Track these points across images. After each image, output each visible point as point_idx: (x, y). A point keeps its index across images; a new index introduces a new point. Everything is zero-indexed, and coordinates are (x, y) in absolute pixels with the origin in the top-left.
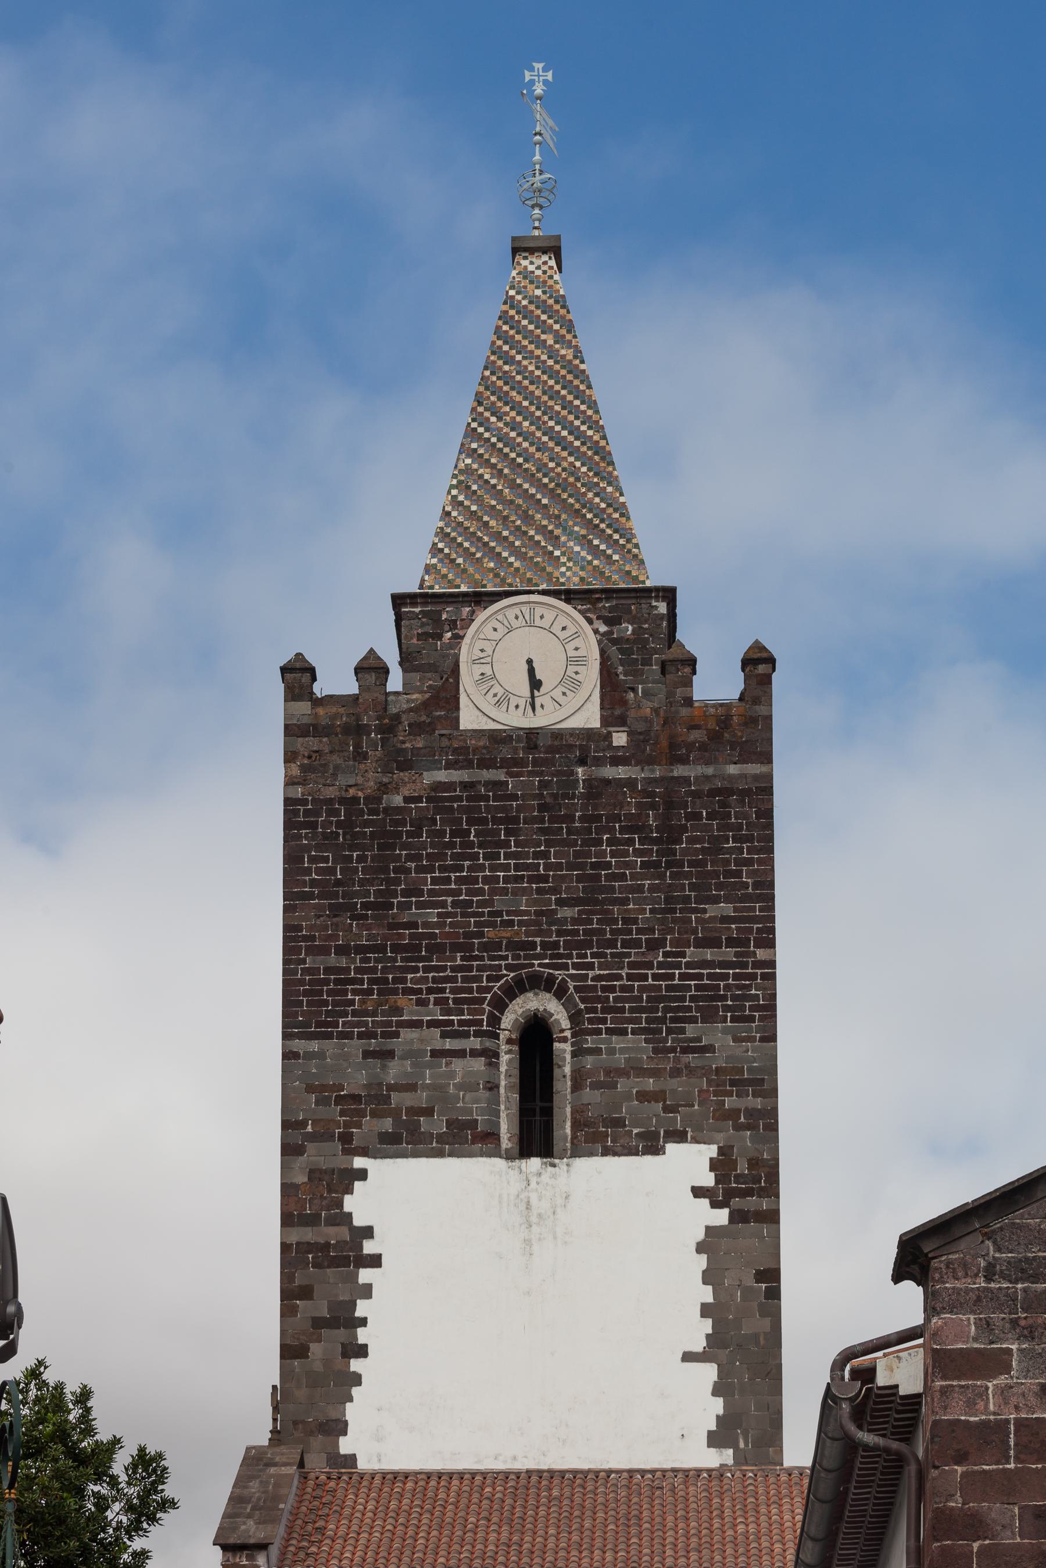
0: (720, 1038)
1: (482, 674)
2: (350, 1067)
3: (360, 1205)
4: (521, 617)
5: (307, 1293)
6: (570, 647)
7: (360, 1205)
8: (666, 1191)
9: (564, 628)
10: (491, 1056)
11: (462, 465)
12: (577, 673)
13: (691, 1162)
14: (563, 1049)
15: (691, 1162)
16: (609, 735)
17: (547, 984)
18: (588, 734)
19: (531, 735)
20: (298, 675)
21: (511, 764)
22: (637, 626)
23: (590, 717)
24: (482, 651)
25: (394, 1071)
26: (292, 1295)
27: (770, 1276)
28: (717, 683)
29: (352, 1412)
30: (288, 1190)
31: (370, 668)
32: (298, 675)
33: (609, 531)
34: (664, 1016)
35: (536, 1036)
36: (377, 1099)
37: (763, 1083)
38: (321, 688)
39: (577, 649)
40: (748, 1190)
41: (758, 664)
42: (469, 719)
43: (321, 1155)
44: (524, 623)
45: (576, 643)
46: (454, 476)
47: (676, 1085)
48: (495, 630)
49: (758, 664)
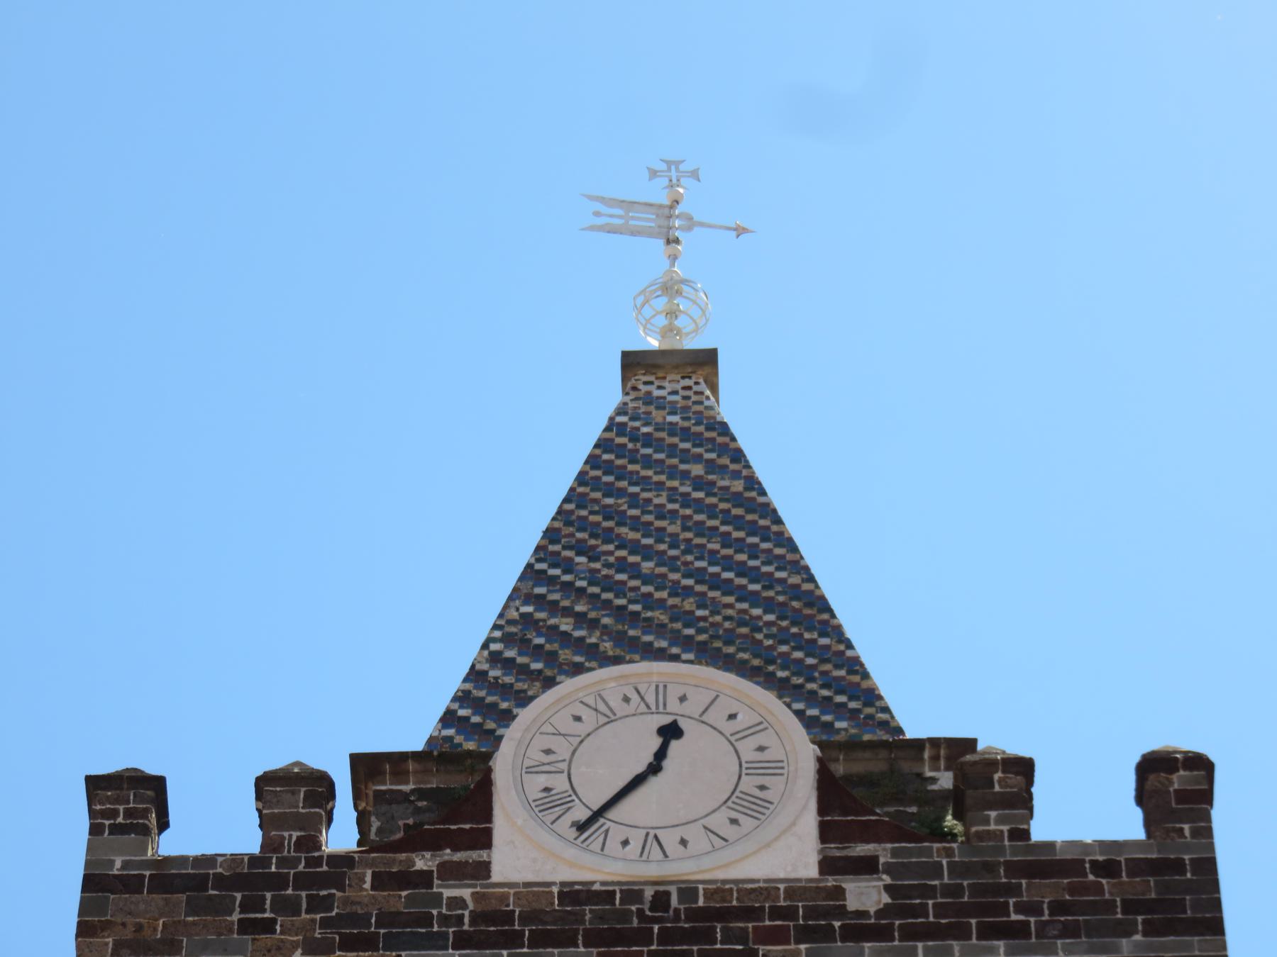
1: (547, 790)
4: (635, 698)
6: (747, 749)
9: (732, 717)
11: (514, 614)
12: (762, 788)
16: (839, 892)
18: (795, 889)
20: (127, 800)
24: (548, 752)
32: (127, 800)
33: (825, 693)
38: (181, 839)
39: (761, 749)
41: (1175, 787)
44: (643, 708)
45: (760, 739)
46: (496, 627)
48: (578, 719)
49: (1175, 787)
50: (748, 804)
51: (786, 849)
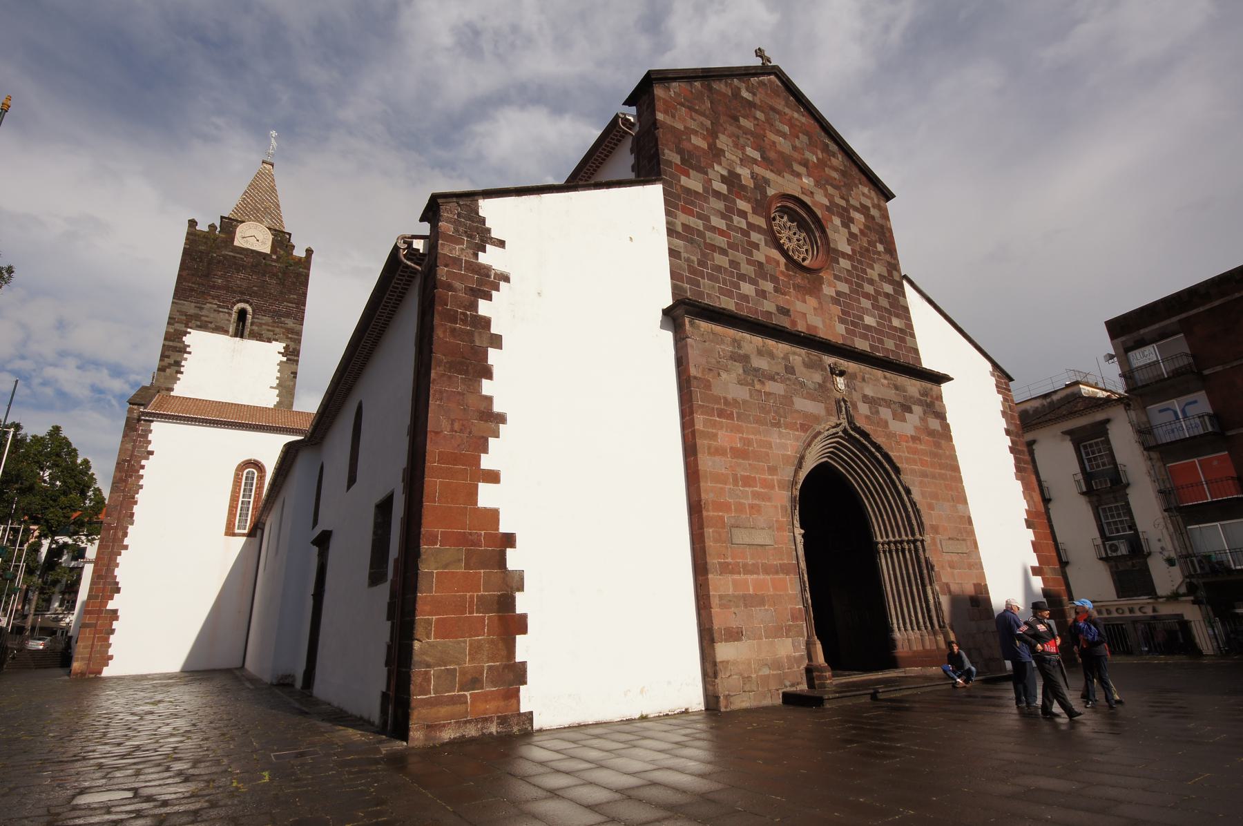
0: (290, 323)
2: (190, 308)
3: (187, 340)
5: (168, 357)
7: (187, 340)
8: (273, 352)
10: (230, 314)
13: (279, 346)
14: (249, 317)
15: (279, 346)
17: (247, 302)
19: (253, 251)
20: (193, 223)
21: (246, 256)
22: (282, 240)
23: (268, 251)
25: (204, 312)
26: (163, 356)
27: (295, 374)
28: (299, 252)
29: (175, 386)
30: (167, 333)
31: (212, 227)
32: (193, 223)
34: (277, 314)
35: (242, 314)
36: (197, 317)
37: (299, 333)
40: (292, 354)
41: (309, 252)
42: (236, 243)
43: (181, 327)
47: (277, 330)
49: (309, 252)
50: (264, 243)
51: (267, 250)
